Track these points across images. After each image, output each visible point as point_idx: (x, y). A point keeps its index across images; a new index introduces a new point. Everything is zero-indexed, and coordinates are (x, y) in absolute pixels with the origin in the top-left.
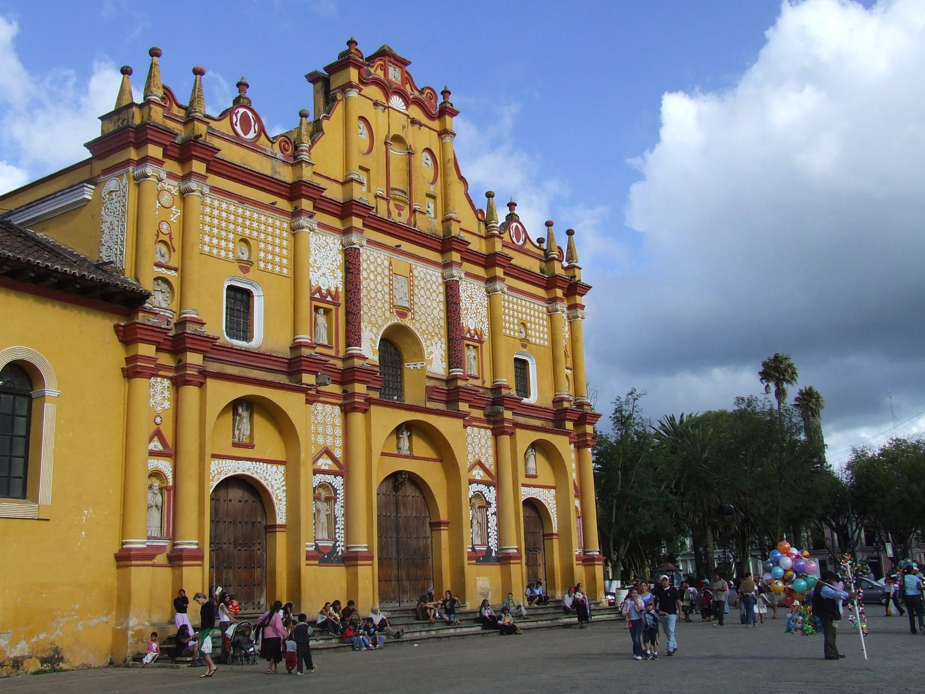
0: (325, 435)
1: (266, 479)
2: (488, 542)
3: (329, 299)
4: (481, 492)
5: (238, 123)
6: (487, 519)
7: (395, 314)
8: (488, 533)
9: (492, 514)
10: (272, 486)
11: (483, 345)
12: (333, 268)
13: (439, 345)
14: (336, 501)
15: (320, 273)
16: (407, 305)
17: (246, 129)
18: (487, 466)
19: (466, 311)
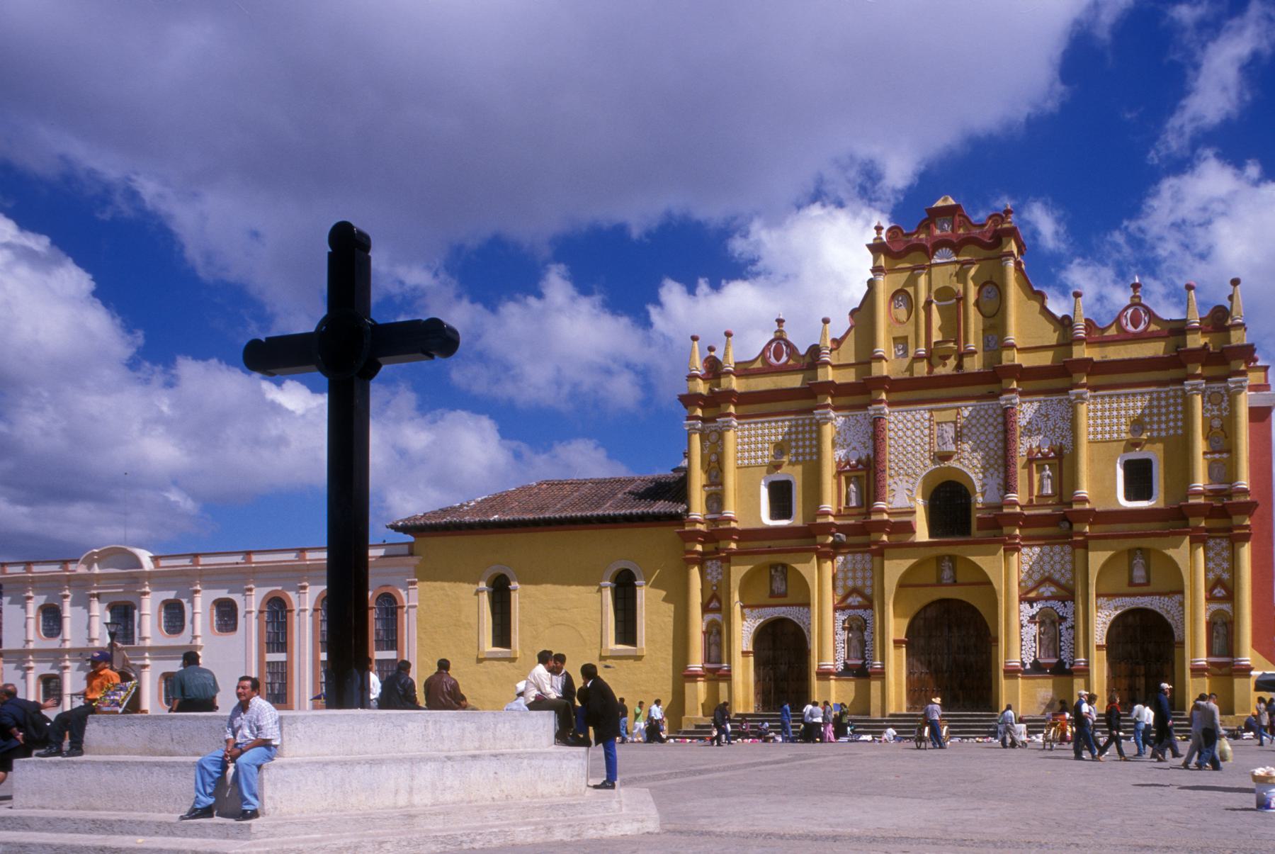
0: (854, 578)
1: (798, 618)
2: (1060, 655)
3: (860, 467)
4: (1052, 608)
5: (772, 356)
6: (1060, 633)
7: (937, 460)
8: (1060, 647)
9: (1067, 629)
10: (804, 623)
11: (1064, 460)
12: (862, 440)
13: (995, 476)
14: (866, 629)
15: (851, 447)
16: (953, 448)
17: (778, 356)
18: (1063, 581)
19: (1037, 432)
